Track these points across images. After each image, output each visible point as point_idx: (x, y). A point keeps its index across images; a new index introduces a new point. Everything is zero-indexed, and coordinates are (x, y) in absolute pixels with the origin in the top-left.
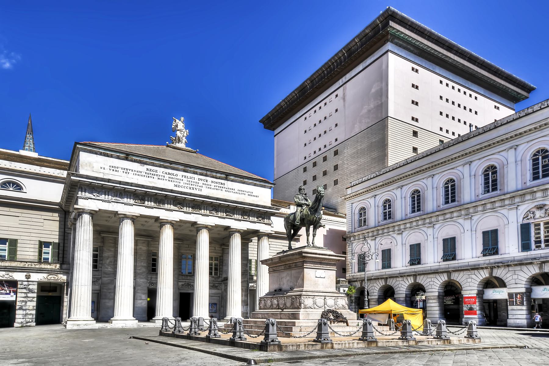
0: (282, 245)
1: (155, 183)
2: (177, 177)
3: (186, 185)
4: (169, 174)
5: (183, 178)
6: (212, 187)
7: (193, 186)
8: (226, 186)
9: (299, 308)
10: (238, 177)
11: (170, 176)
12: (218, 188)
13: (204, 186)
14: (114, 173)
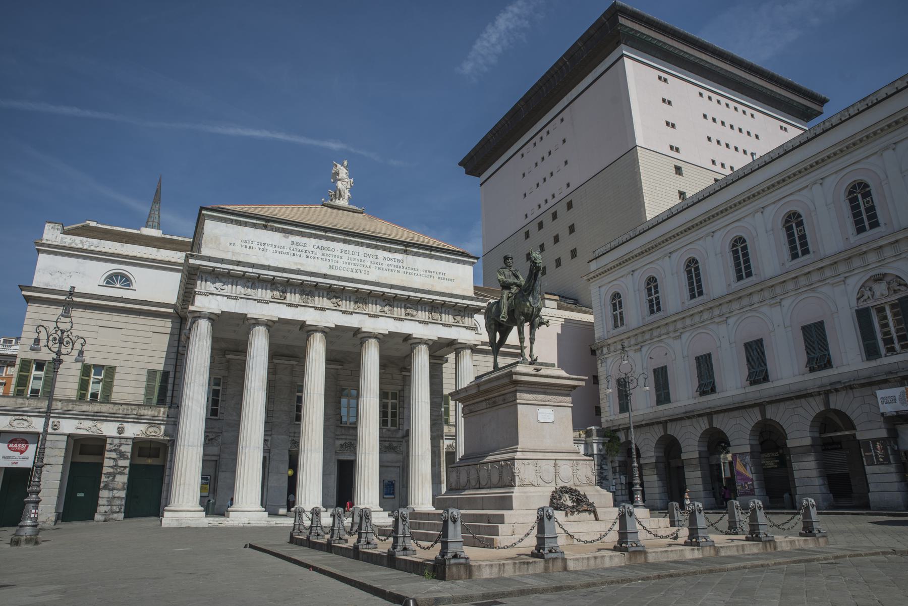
0: (486, 364)
1: (302, 264)
2: (334, 253)
3: (347, 266)
4: (323, 248)
5: (343, 254)
6: (385, 267)
8: (405, 265)
9: (511, 485)
10: (423, 249)
11: (325, 252)
12: (393, 268)
13: (372, 265)
14: (248, 251)
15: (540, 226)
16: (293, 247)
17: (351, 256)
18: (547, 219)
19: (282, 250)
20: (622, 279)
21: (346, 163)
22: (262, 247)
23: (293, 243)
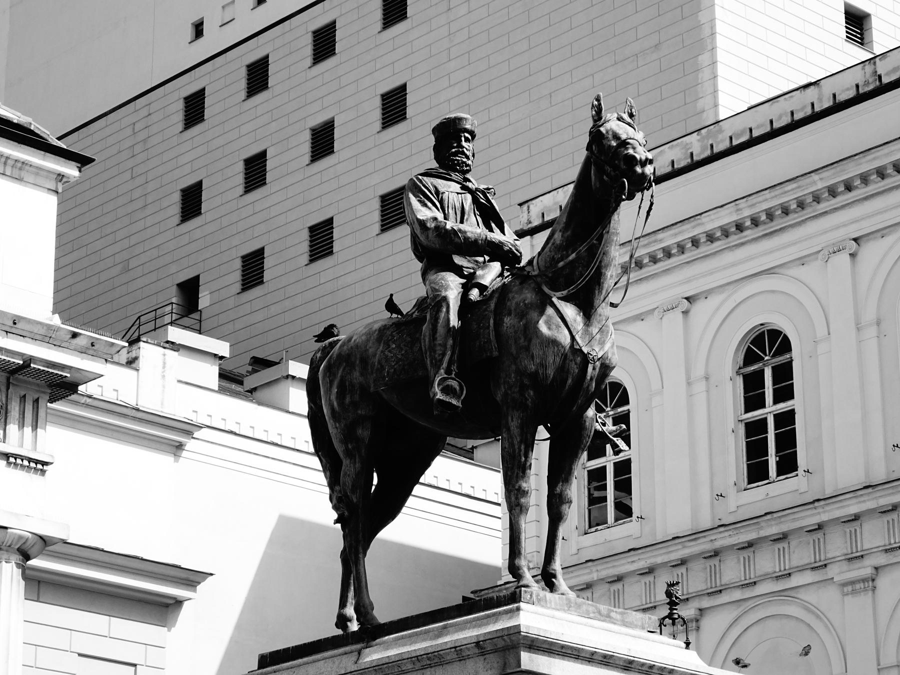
15: (258, 77)
18: (290, 53)
20: (637, 328)
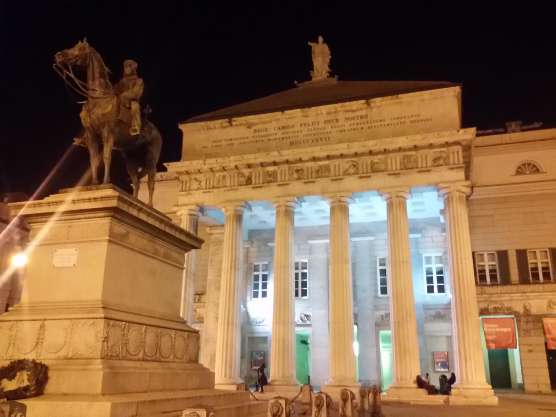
2: (294, 130)
3: (307, 138)
4: (284, 128)
6: (347, 127)
7: (316, 137)
12: (355, 127)
13: (334, 130)
16: (257, 134)
17: (311, 127)
19: (247, 140)
21: (321, 39)
22: (229, 142)
23: (255, 131)
